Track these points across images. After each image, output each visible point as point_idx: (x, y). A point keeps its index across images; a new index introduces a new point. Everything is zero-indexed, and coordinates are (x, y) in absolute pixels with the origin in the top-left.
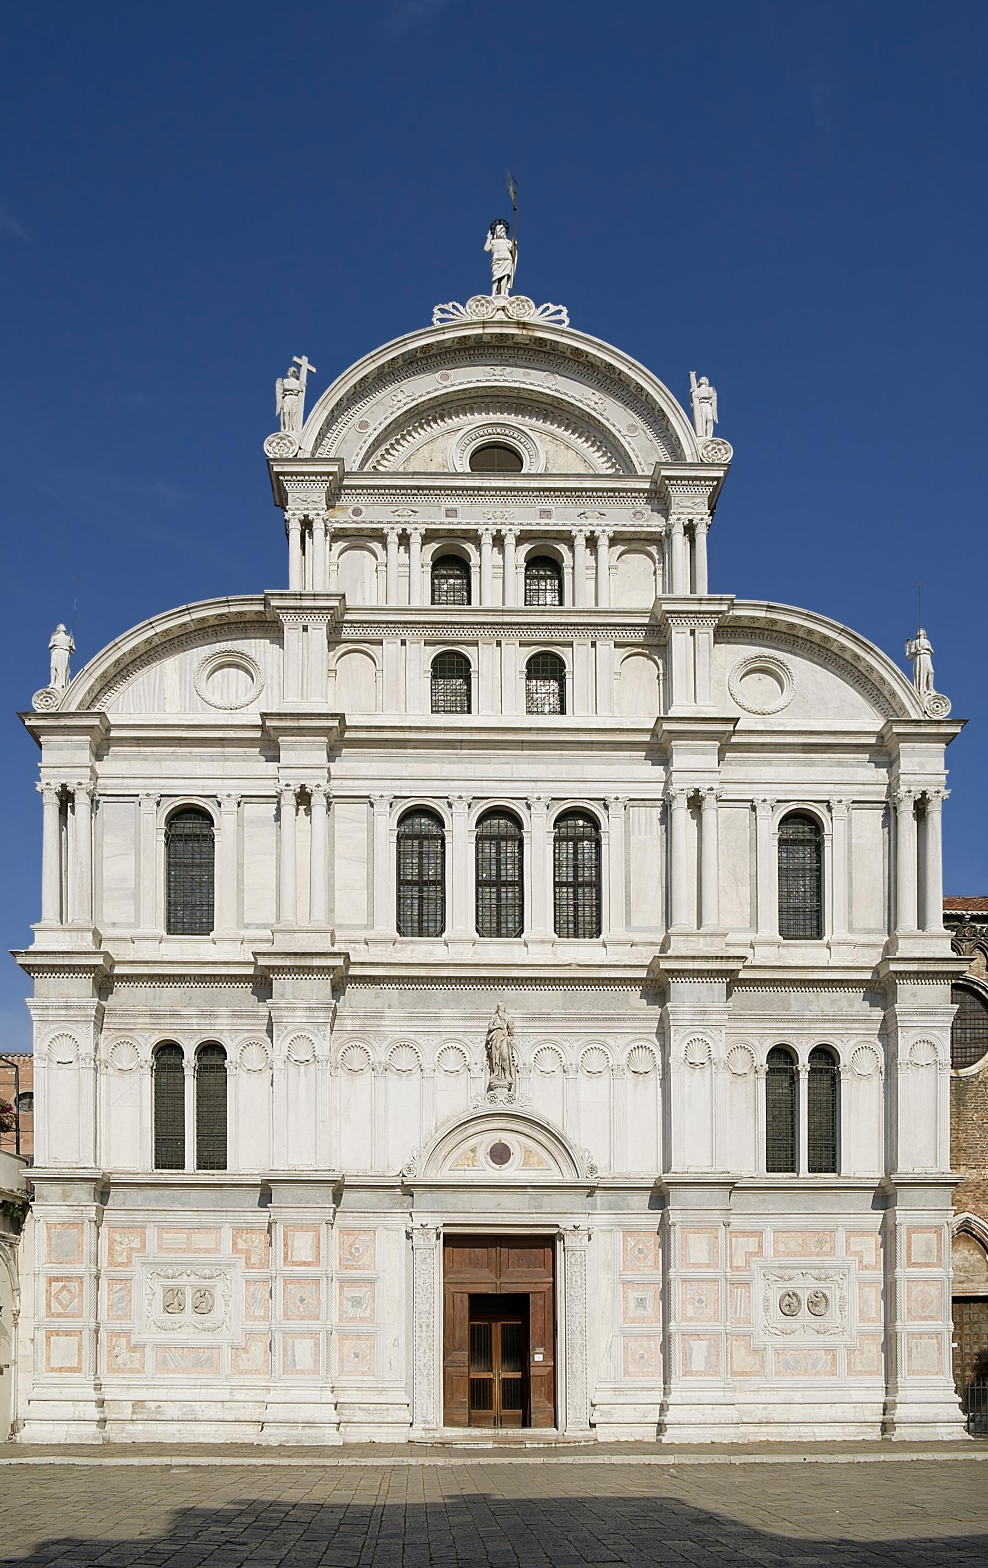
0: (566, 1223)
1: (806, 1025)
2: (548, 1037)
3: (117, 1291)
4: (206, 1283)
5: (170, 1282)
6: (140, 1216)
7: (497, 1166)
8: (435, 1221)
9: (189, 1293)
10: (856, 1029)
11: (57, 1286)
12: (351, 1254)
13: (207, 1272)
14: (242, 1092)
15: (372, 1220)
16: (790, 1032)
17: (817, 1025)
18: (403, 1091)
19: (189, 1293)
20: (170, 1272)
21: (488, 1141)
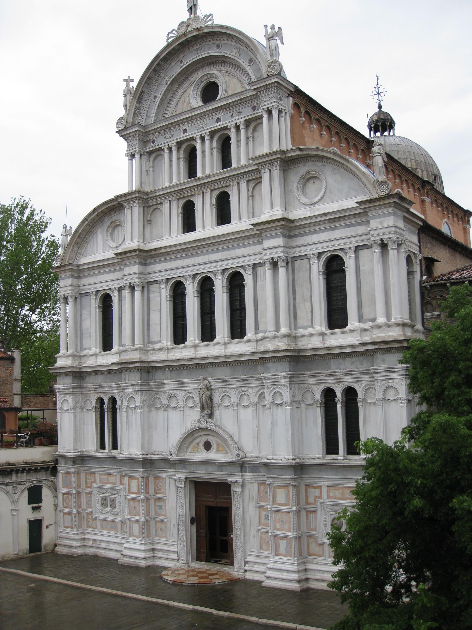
0: (231, 479)
1: (338, 378)
2: (225, 390)
7: (206, 451)
8: (183, 476)
9: (109, 500)
10: (364, 378)
11: (65, 496)
12: (158, 487)
13: (114, 492)
14: (122, 416)
15: (164, 474)
16: (331, 381)
17: (344, 377)
18: (174, 416)
19: (109, 500)
21: (204, 439)
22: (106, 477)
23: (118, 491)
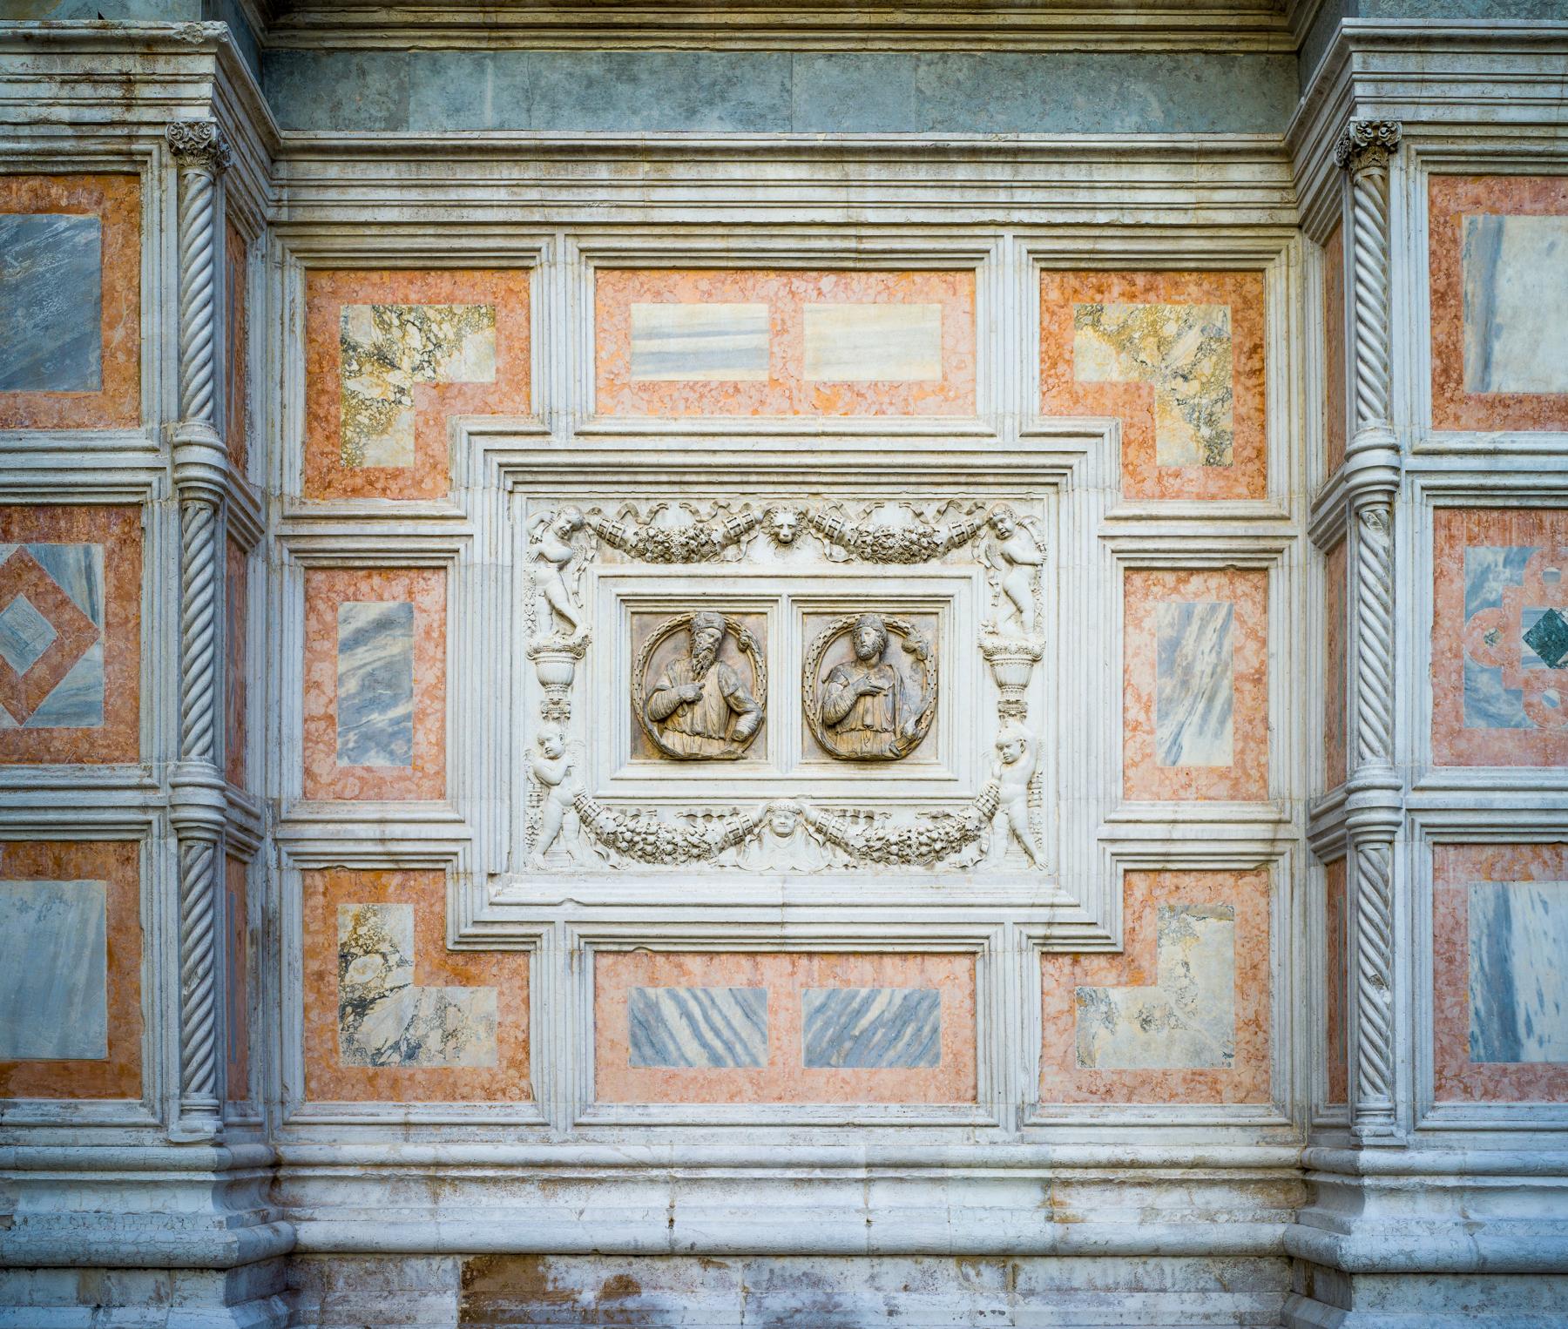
3: (360, 638)
4: (894, 581)
5: (675, 580)
6: (490, 194)
9: (786, 642)
13: (893, 519)
19: (786, 642)
20: (675, 522)
22: (759, 311)
23: (980, 493)
